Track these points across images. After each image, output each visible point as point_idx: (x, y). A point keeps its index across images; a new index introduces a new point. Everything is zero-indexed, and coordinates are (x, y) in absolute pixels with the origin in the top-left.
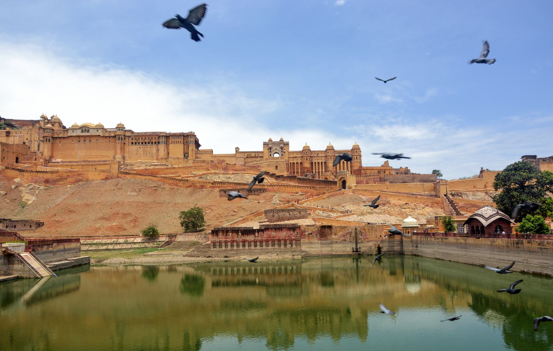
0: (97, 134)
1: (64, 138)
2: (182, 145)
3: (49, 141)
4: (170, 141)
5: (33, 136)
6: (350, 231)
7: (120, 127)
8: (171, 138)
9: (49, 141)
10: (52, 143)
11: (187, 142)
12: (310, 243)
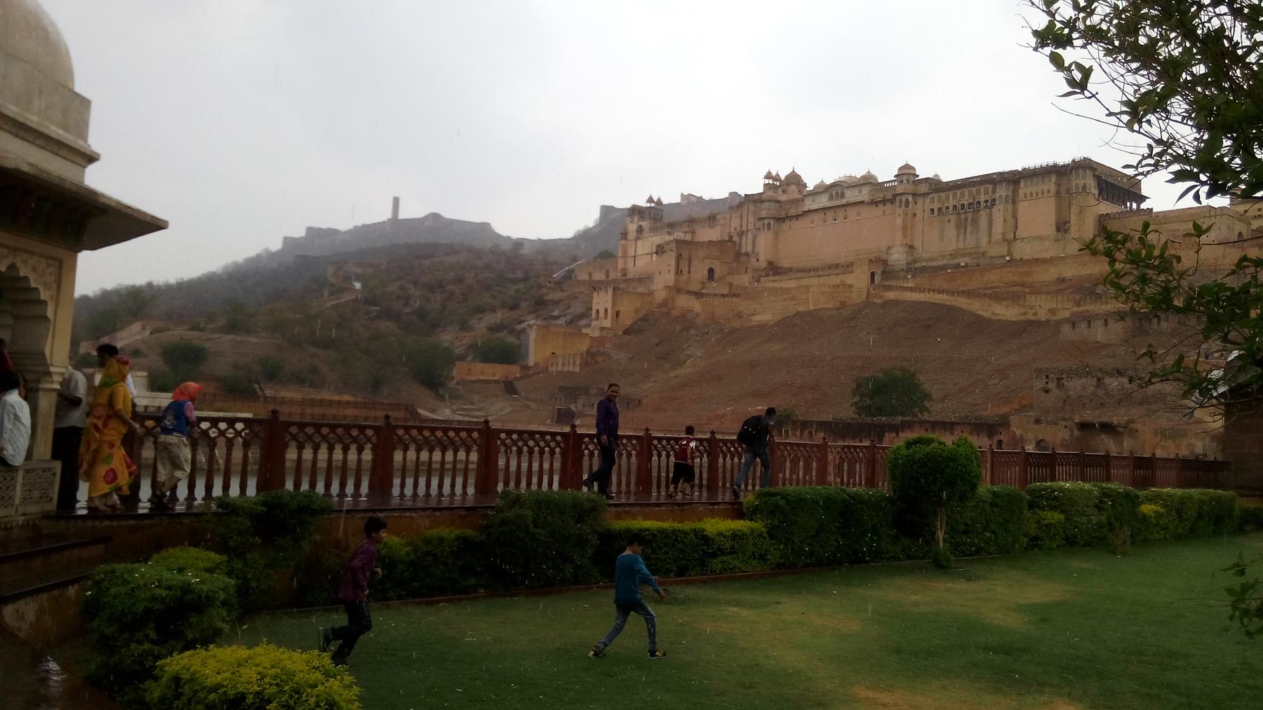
0: (860, 199)
2: (1053, 200)
3: (769, 229)
4: (1021, 192)
5: (745, 220)
7: (906, 173)
8: (1022, 184)
9: (769, 229)
10: (777, 234)
11: (1068, 191)
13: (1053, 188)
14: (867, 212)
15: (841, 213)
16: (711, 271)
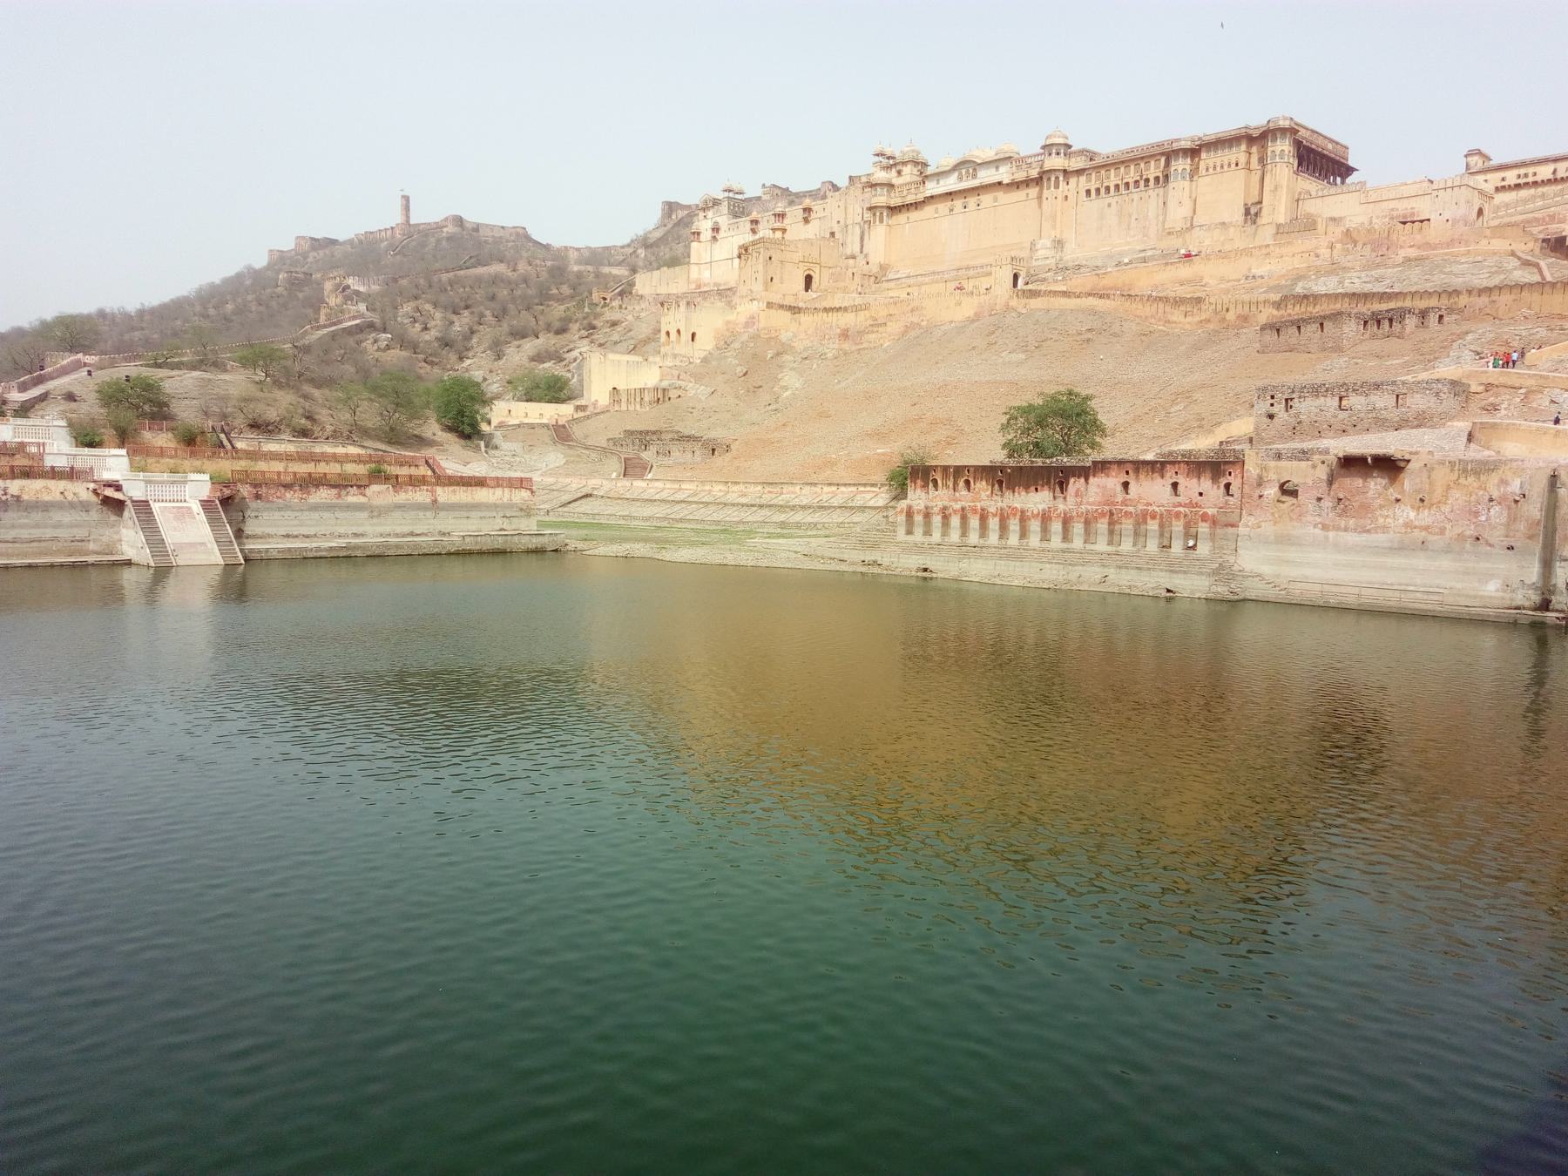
0: (996, 179)
1: (916, 205)
3: (881, 221)
4: (1202, 165)
6: (1515, 487)
8: (1204, 155)
9: (881, 221)
12: (1283, 540)
13: (1243, 158)
14: (1003, 197)
15: (972, 201)
16: (809, 279)
